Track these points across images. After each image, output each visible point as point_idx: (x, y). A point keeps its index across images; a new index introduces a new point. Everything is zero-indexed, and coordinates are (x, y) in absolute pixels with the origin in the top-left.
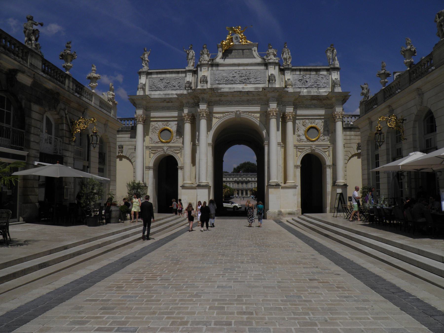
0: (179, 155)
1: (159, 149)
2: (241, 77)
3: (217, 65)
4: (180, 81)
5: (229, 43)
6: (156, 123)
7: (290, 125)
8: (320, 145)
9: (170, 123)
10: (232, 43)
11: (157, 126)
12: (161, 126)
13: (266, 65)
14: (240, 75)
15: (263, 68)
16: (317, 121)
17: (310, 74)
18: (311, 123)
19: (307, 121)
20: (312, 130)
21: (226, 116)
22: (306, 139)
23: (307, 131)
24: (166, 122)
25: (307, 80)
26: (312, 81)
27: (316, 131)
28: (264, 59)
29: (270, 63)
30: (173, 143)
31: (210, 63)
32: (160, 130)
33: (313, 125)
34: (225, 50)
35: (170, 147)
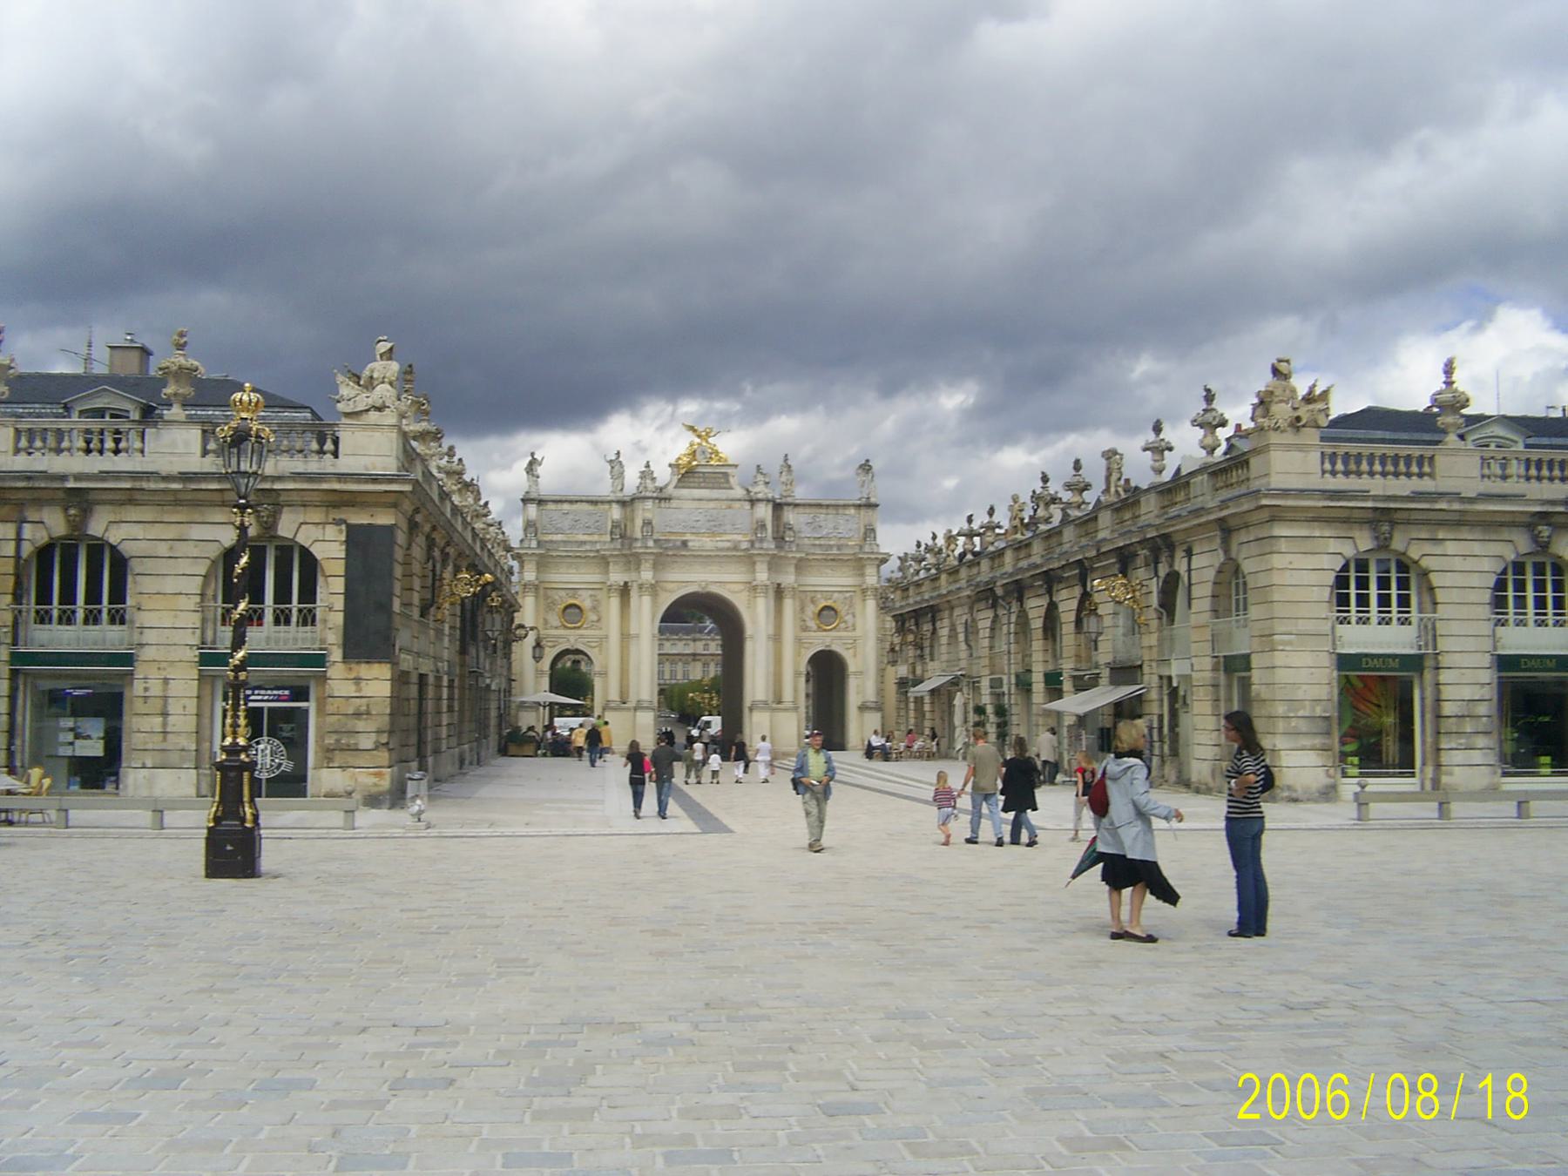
0: (596, 650)
1: (561, 640)
2: (709, 521)
3: (668, 499)
4: (598, 518)
5: (690, 463)
6: (555, 591)
7: (789, 605)
8: (840, 638)
9: (580, 592)
10: (695, 463)
11: (557, 597)
12: (565, 599)
13: (753, 502)
14: (708, 518)
15: (747, 506)
16: (836, 595)
17: (827, 514)
18: (826, 599)
19: (819, 596)
20: (825, 613)
21: (679, 589)
22: (815, 628)
23: (817, 612)
24: (572, 591)
25: (823, 524)
26: (831, 526)
27: (832, 613)
28: (747, 490)
29: (759, 500)
30: (586, 628)
31: (655, 495)
32: (564, 605)
33: (829, 603)
34: (683, 475)
35: (582, 636)
